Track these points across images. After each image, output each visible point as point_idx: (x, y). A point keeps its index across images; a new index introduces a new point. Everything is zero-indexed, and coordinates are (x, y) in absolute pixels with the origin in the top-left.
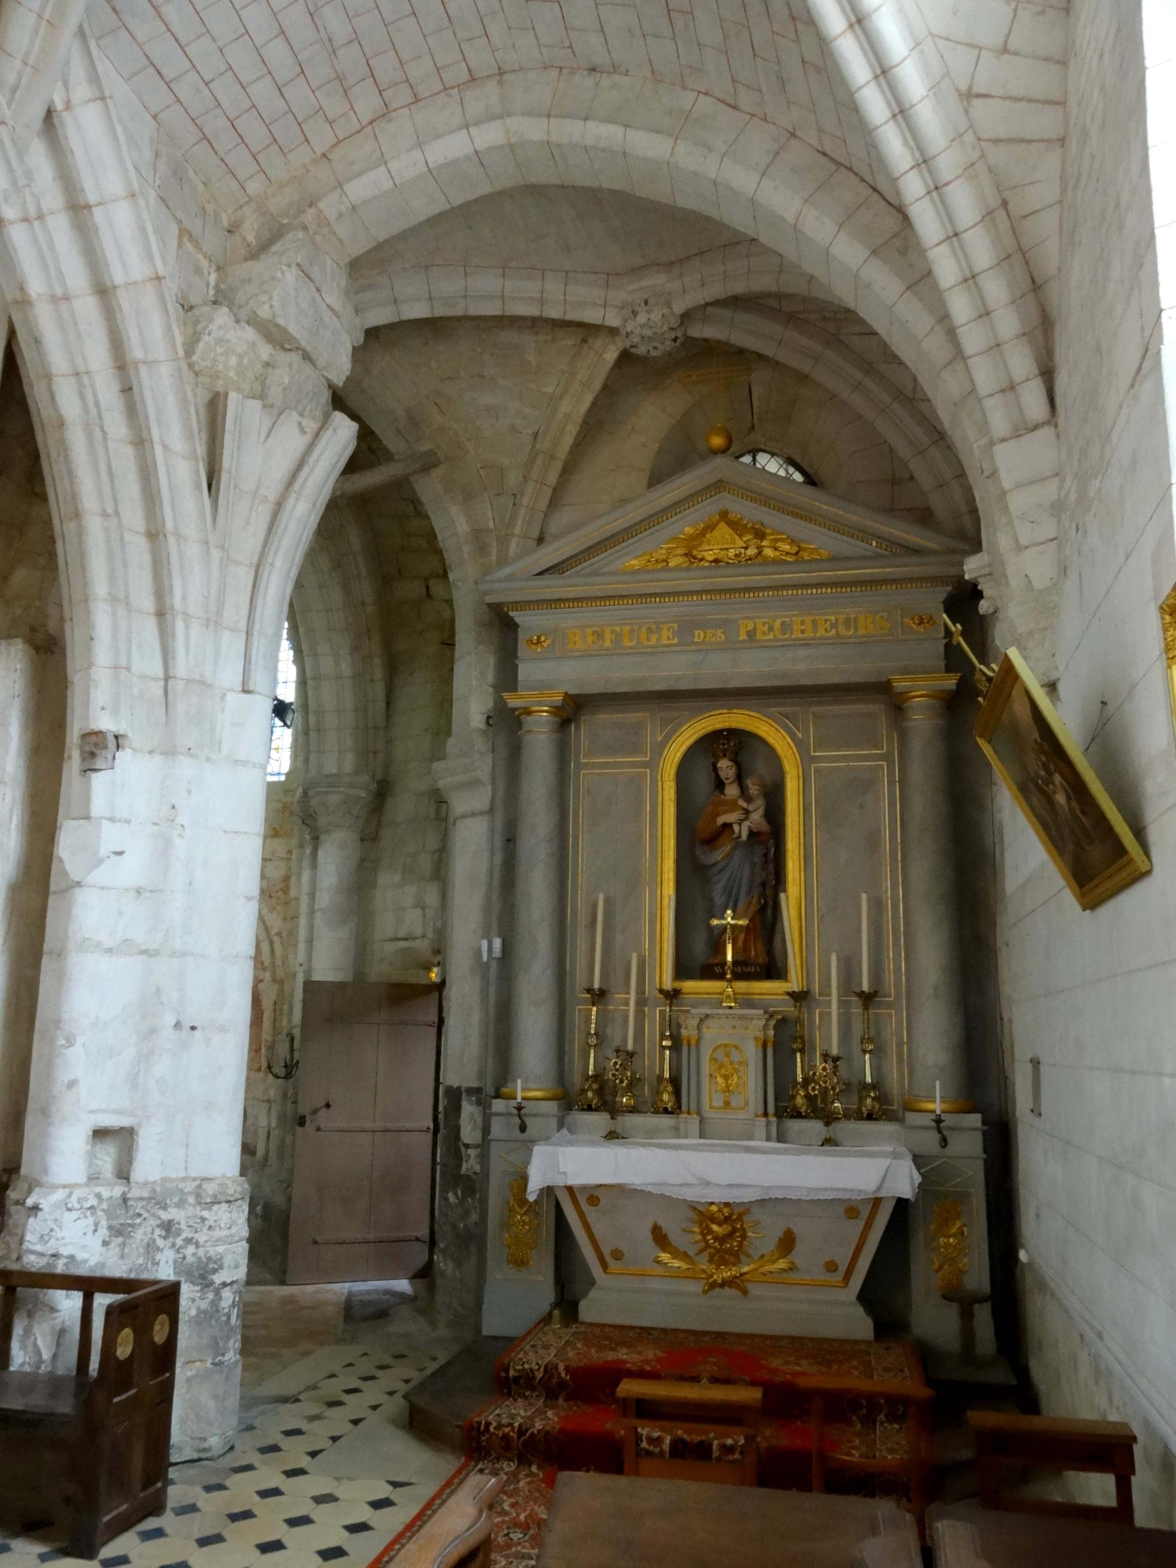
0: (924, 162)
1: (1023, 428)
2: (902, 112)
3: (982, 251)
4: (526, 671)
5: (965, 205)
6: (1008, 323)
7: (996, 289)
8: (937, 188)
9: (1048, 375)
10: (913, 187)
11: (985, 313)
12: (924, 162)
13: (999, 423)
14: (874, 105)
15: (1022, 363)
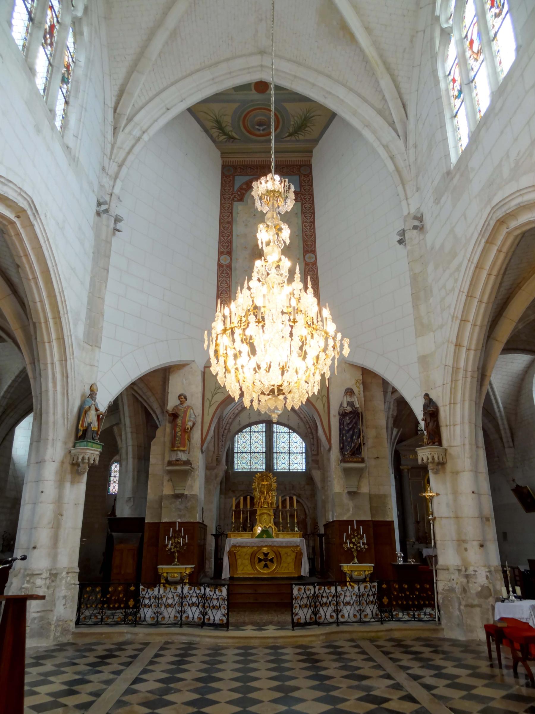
0: (501, 416)
1: (510, 447)
2: (500, 411)
3: (507, 426)
4: (403, 462)
5: (505, 422)
6: (509, 434)
7: (508, 431)
8: (502, 419)
9: (513, 441)
10: (499, 418)
11: (506, 433)
12: (501, 416)
13: (506, 445)
14: (496, 410)
15: (510, 440)
